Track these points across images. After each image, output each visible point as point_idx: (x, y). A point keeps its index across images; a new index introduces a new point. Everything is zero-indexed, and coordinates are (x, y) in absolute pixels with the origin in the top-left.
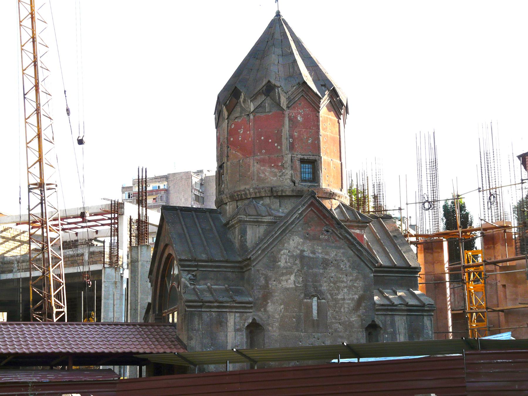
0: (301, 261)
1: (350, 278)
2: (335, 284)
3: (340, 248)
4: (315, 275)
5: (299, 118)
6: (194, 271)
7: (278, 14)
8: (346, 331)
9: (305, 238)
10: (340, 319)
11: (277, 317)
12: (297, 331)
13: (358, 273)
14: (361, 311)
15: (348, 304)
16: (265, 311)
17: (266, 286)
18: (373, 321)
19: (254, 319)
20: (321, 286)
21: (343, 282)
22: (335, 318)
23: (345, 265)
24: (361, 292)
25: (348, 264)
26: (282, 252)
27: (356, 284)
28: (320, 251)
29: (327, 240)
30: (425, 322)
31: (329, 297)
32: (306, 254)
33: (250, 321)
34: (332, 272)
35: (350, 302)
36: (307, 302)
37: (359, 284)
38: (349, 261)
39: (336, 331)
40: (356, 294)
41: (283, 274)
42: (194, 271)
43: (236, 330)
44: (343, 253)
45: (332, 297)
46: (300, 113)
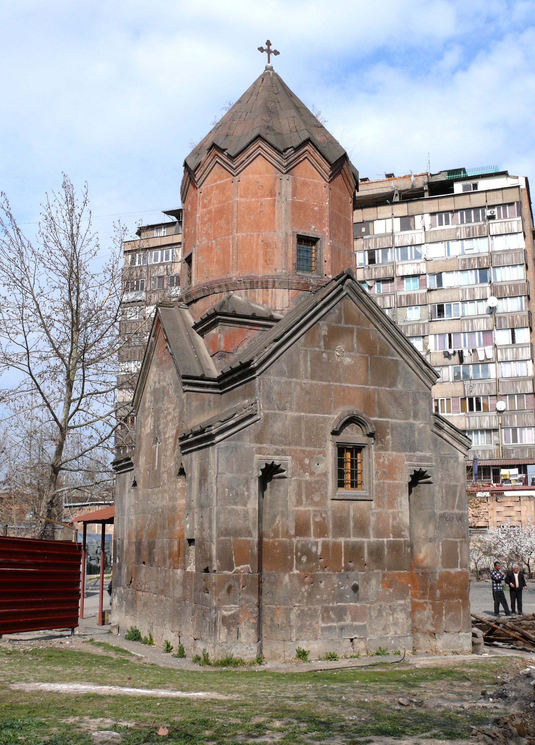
7: (269, 69)
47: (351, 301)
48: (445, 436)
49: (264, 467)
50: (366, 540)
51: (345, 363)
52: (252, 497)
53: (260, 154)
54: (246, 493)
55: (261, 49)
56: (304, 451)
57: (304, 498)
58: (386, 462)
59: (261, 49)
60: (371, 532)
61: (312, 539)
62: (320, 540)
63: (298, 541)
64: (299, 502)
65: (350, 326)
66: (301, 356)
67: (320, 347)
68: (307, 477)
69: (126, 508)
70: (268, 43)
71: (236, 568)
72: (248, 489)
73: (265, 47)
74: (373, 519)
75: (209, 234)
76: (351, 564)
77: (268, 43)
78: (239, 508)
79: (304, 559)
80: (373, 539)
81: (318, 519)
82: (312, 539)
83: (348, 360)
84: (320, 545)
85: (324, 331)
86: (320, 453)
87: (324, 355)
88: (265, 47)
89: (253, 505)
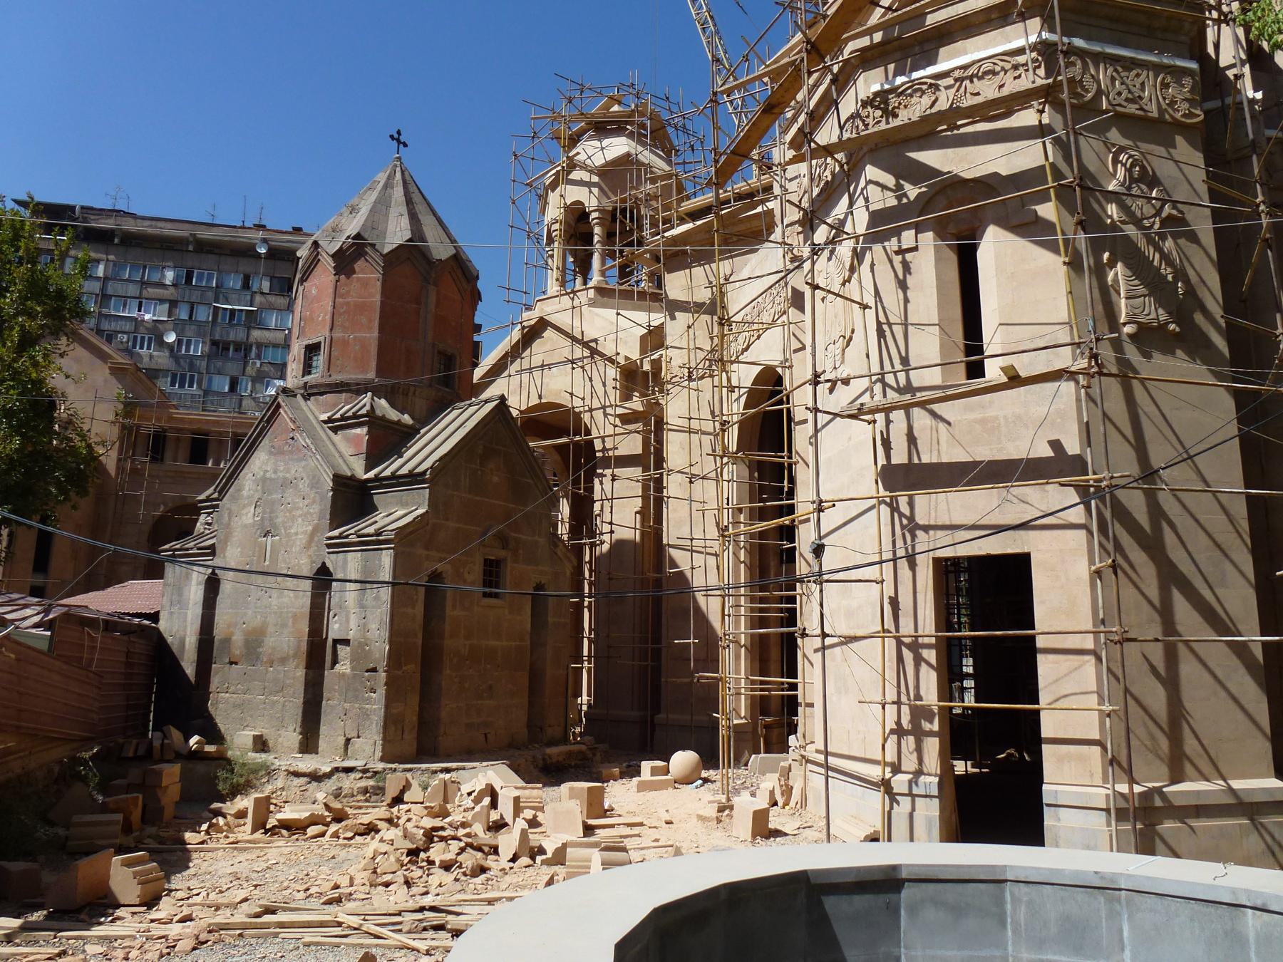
1: (306, 502)
3: (300, 460)
4: (273, 503)
9: (271, 453)
14: (314, 548)
15: (301, 539)
18: (324, 563)
21: (298, 509)
22: (285, 561)
23: (303, 486)
29: (291, 452)
32: (268, 475)
34: (289, 495)
37: (315, 509)
41: (244, 507)
43: (198, 584)
55: (392, 137)
59: (392, 137)
64: (454, 607)
70: (399, 133)
73: (396, 136)
77: (399, 133)
78: (410, 610)
80: (505, 643)
83: (496, 479)
88: (396, 136)
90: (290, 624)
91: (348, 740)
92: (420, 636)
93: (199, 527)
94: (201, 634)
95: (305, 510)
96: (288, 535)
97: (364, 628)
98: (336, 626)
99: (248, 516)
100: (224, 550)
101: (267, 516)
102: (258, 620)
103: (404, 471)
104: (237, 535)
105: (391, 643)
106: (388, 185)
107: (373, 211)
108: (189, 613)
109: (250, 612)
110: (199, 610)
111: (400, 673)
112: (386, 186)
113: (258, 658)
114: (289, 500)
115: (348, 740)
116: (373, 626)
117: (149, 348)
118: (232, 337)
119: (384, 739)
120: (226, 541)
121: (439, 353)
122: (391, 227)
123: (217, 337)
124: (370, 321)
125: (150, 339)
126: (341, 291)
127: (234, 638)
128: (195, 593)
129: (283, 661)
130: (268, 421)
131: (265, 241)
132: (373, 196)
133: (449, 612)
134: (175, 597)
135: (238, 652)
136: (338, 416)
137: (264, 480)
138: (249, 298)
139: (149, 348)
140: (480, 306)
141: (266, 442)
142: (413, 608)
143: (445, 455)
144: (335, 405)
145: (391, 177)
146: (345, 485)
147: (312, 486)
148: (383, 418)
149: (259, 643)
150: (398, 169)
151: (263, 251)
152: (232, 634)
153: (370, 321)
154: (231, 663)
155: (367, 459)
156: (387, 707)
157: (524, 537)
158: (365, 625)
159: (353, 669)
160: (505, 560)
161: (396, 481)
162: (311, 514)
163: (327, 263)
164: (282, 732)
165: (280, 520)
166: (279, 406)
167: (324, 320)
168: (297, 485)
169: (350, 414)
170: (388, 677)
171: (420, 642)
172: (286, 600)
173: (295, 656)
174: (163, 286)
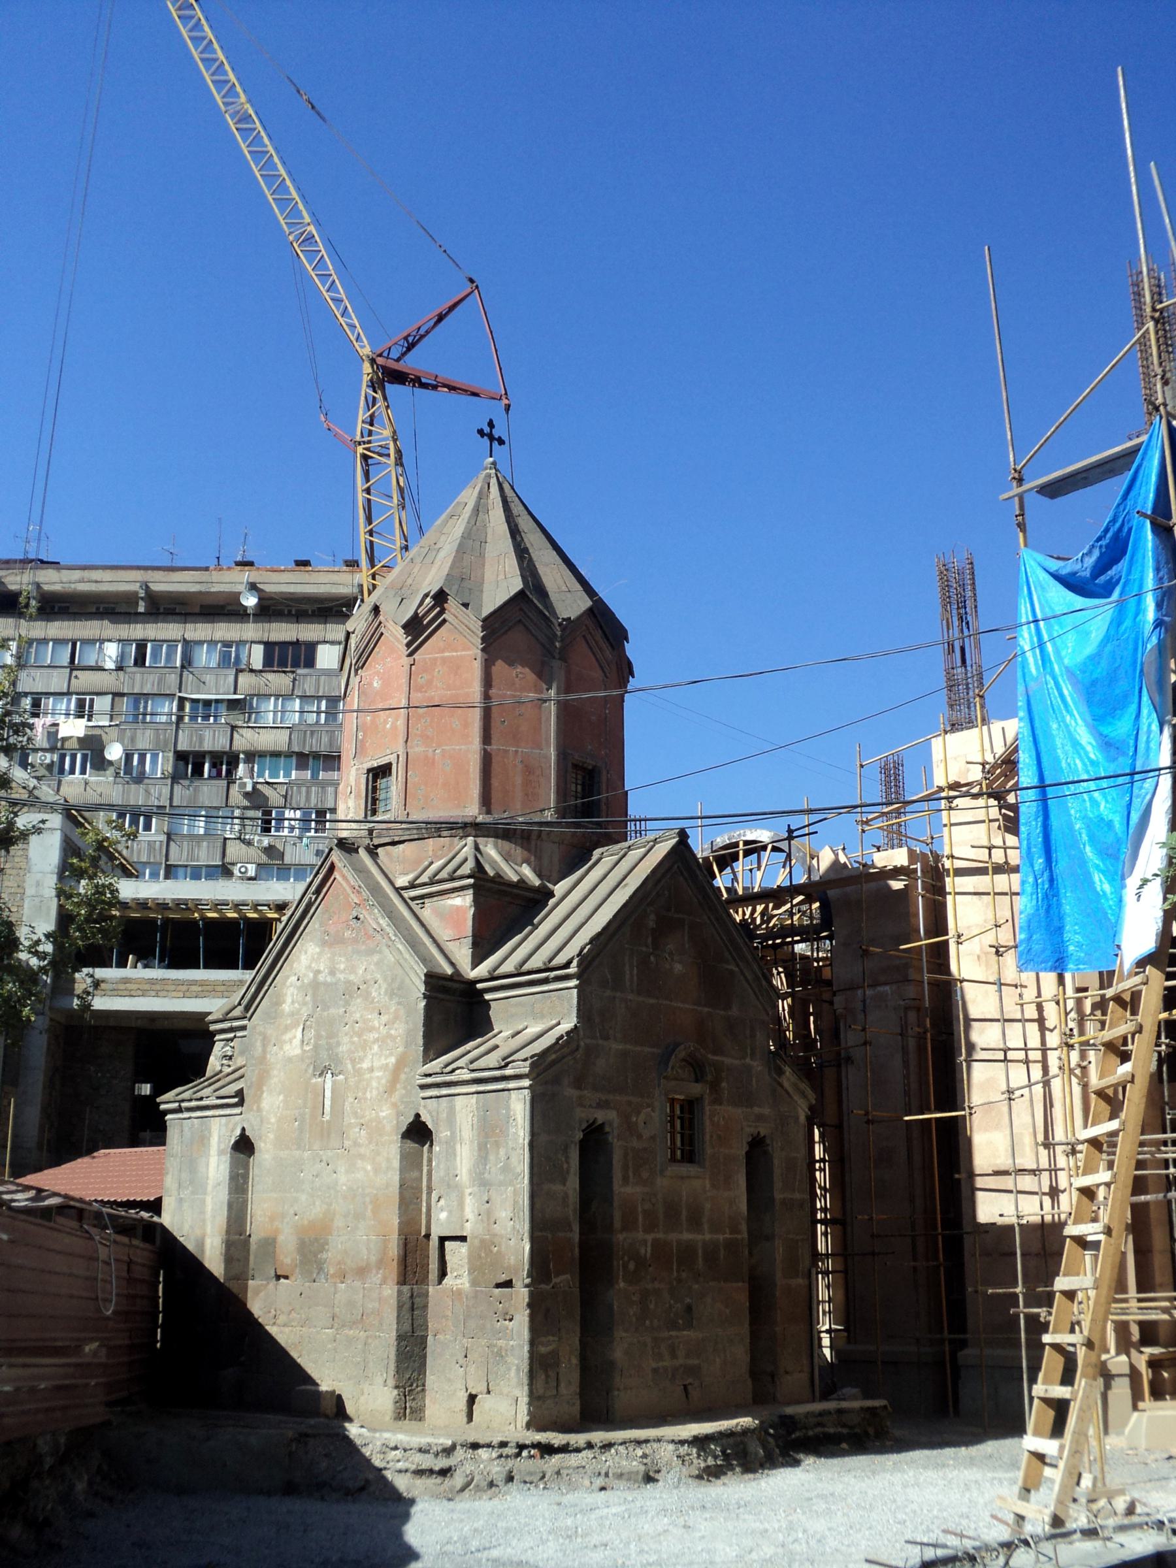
0: (314, 995)
1: (384, 1018)
2: (360, 1036)
3: (370, 952)
5: (375, 685)
6: (232, 1040)
8: (370, 1143)
9: (324, 943)
10: (363, 1117)
11: (273, 1120)
12: (299, 1148)
13: (399, 1003)
14: (400, 1091)
16: (259, 1110)
17: (263, 1059)
18: (418, 1116)
19: (243, 1129)
20: (338, 1044)
23: (378, 993)
24: (401, 1049)
25: (384, 986)
26: (288, 983)
27: (393, 1032)
28: (342, 966)
29: (355, 941)
30: (512, 1106)
31: (350, 1066)
32: (321, 978)
33: (238, 1132)
35: (380, 1074)
36: (316, 1083)
38: (385, 980)
39: (356, 1144)
40: (391, 1054)
41: (287, 1029)
42: (232, 1040)
43: (221, 1153)
44: (377, 964)
45: (354, 1067)
46: (378, 673)
47: (681, 879)
48: (786, 1084)
49: (584, 1126)
50: (700, 1237)
51: (676, 971)
52: (572, 1170)
53: (520, 621)
54: (565, 1166)
55: (481, 432)
56: (630, 1103)
57: (631, 1174)
58: (722, 1123)
59: (481, 432)
60: (706, 1227)
61: (640, 1235)
62: (650, 1237)
63: (625, 1239)
64: (625, 1179)
65: (681, 916)
66: (627, 958)
67: (647, 946)
68: (635, 1143)
69: (211, 1182)
70: (491, 424)
71: (554, 1280)
72: (567, 1157)
73: (487, 430)
74: (708, 1206)
75: (428, 737)
76: (684, 1275)
77: (491, 424)
78: (557, 1188)
79: (632, 1266)
80: (708, 1237)
81: (647, 1206)
82: (640, 1235)
84: (649, 1244)
85: (651, 922)
86: (648, 1106)
87: (652, 958)
88: (487, 430)
89: (574, 1182)
90: (369, 1213)
91: (472, 1399)
92: (576, 1228)
93: (214, 1063)
94: (228, 1232)
95: (383, 1030)
96: (358, 1072)
97: (487, 1215)
98: (443, 1216)
99: (293, 1044)
100: (258, 1099)
101: (323, 1042)
102: (317, 1210)
103: (536, 962)
104: (277, 1077)
105: (533, 1240)
106: (479, 509)
107: (461, 550)
108: (209, 1200)
109: (303, 1197)
110: (223, 1195)
111: (548, 1287)
112: (477, 510)
113: (320, 1269)
114: (357, 1016)
115: (472, 1399)
116: (503, 1214)
117: (83, 772)
118: (207, 746)
119: (531, 1394)
120: (259, 1087)
121: (575, 766)
122: (489, 574)
123: (183, 746)
124: (466, 725)
125: (84, 758)
126: (420, 680)
127: (281, 1238)
128: (216, 1166)
129: (362, 1272)
130: (318, 892)
131: (253, 587)
132: (458, 529)
133: (617, 1186)
134: (184, 1175)
135: (288, 1261)
136: (424, 878)
137: (315, 985)
138: (231, 678)
139: (83, 772)
140: (633, 683)
141: (314, 926)
142: (564, 1185)
143: (599, 935)
144: (419, 862)
145: (482, 496)
146: (446, 990)
147: (391, 994)
148: (499, 879)
149: (322, 1246)
150: (494, 481)
151: (250, 601)
152: (277, 1231)
153: (466, 725)
154: (278, 1277)
155: (475, 945)
156: (532, 1343)
157: (728, 1061)
158: (489, 1213)
159: (474, 1283)
160: (700, 1099)
161: (524, 978)
162: (393, 1038)
163: (395, 636)
164: (366, 1387)
165: (343, 1048)
166: (332, 868)
167: (394, 727)
168: (369, 994)
169: (444, 874)
170: (531, 1294)
171: (576, 1236)
172: (359, 1175)
173: (380, 1263)
174: (100, 669)
